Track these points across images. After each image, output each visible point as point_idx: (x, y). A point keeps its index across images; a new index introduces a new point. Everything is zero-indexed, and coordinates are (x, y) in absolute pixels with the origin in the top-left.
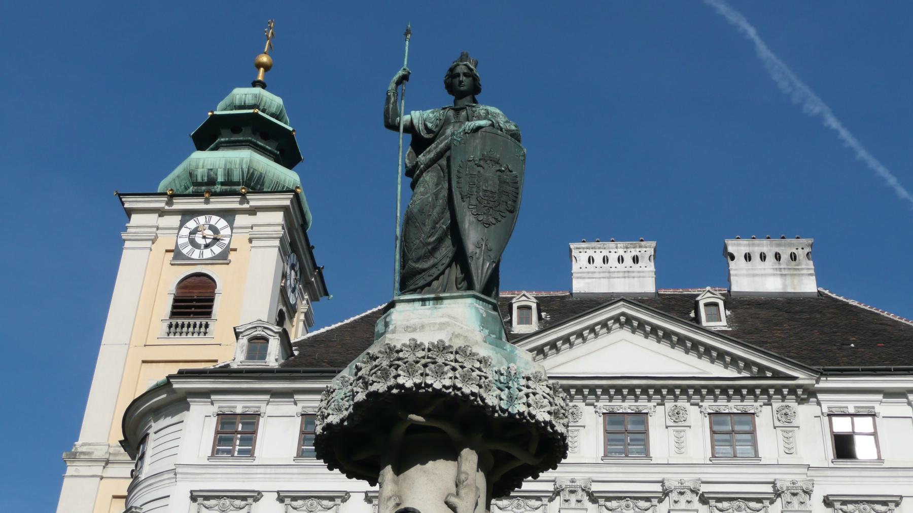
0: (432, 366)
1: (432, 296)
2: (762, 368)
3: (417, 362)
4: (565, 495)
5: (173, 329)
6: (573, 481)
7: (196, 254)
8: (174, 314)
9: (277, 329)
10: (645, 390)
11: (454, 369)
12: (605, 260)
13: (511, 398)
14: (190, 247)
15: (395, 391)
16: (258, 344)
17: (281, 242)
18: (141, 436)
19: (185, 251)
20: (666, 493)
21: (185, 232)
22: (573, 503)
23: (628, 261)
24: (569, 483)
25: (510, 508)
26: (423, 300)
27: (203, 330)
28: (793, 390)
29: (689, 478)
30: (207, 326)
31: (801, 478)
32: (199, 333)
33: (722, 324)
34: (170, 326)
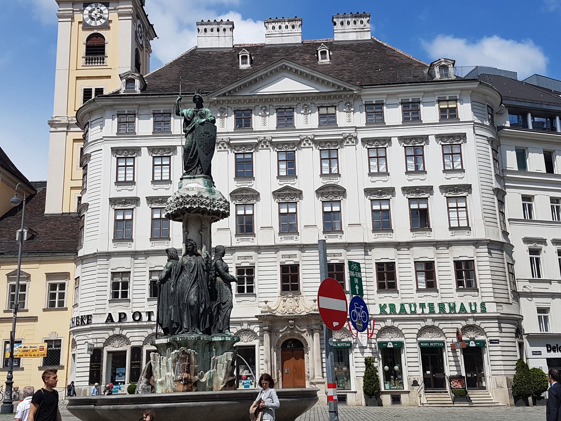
2: (339, 87)
5: (88, 61)
6: (265, 138)
7: (93, 24)
8: (87, 54)
9: (137, 75)
12: (280, 27)
14: (90, 20)
16: (130, 81)
17: (133, 17)
18: (85, 122)
19: (88, 22)
21: (86, 12)
23: (290, 28)
26: (190, 178)
27: (102, 61)
28: (352, 96)
29: (310, 134)
30: (103, 59)
31: (352, 132)
32: (100, 63)
33: (327, 61)
34: (86, 60)
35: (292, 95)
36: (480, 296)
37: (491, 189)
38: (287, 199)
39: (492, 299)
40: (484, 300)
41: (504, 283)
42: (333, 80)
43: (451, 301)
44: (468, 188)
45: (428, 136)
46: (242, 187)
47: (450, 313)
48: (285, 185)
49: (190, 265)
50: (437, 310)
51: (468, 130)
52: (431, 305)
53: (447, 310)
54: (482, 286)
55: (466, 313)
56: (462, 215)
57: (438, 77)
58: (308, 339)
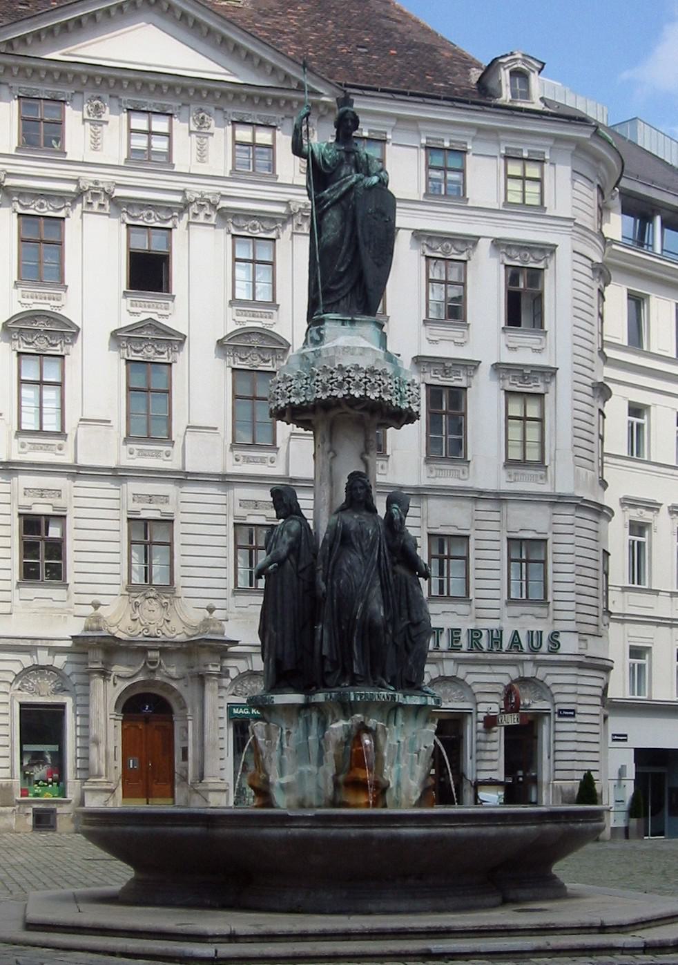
0: (369, 384)
1: (350, 318)
3: (360, 380)
4: (88, 198)
6: (96, 183)
10: (171, 88)
11: (380, 385)
13: (402, 398)
15: (347, 398)
20: (185, 206)
22: (95, 208)
24: (92, 185)
25: (33, 206)
35: (171, 80)
36: (550, 619)
37: (589, 382)
38: (149, 353)
39: (572, 626)
40: (559, 626)
41: (592, 591)
42: (274, 57)
43: (494, 625)
44: (549, 373)
45: (479, 237)
46: (35, 307)
47: (490, 651)
48: (144, 317)
49: (361, 533)
50: (464, 642)
51: (564, 242)
52: (455, 632)
53: (484, 643)
54: (559, 596)
55: (521, 652)
56: (533, 433)
57: (506, 96)
58: (188, 692)
